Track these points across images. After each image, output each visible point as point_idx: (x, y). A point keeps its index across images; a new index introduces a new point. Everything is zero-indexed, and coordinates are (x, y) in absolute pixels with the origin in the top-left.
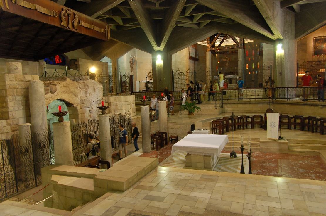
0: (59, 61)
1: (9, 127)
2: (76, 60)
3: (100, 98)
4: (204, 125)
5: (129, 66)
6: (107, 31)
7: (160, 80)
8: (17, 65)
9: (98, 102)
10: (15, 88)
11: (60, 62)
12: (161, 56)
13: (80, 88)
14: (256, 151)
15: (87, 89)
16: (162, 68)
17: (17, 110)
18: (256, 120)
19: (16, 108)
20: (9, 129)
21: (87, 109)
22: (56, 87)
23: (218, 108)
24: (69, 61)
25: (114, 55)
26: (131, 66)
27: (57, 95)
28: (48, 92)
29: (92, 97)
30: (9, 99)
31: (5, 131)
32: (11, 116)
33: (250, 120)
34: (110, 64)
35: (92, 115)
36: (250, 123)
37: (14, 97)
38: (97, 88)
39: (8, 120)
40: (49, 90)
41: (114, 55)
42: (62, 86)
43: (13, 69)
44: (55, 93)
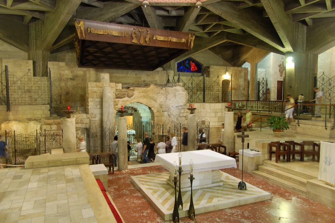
0: (195, 69)
1: (88, 120)
2: (208, 67)
3: (182, 104)
4: (257, 145)
5: (278, 71)
6: (189, 41)
7: (291, 87)
8: (104, 76)
9: (180, 108)
10: (95, 92)
11: (196, 70)
12: (293, 58)
13: (161, 93)
14: (301, 193)
15: (168, 95)
16: (294, 72)
17: (95, 109)
18: (306, 148)
19: (95, 107)
20: (87, 121)
21: (166, 113)
22: (133, 93)
23: (329, 128)
24: (204, 68)
25: (253, 59)
26: (280, 71)
27: (134, 99)
28: (124, 96)
29: (171, 102)
30: (90, 100)
31: (85, 122)
32: (90, 112)
33: (298, 148)
34: (249, 69)
35: (170, 119)
36: (297, 152)
37: (94, 99)
38: (178, 95)
39: (88, 115)
40: (126, 95)
41: (253, 59)
42: (141, 91)
43: (102, 78)
44: (132, 98)
